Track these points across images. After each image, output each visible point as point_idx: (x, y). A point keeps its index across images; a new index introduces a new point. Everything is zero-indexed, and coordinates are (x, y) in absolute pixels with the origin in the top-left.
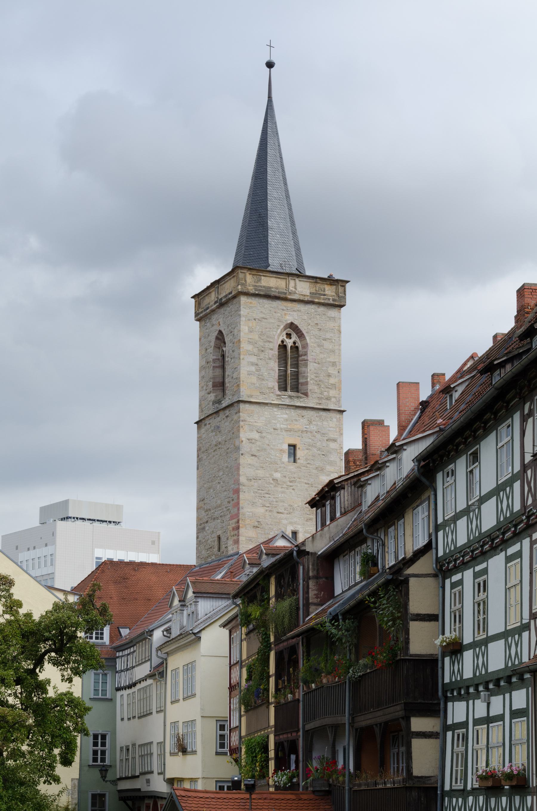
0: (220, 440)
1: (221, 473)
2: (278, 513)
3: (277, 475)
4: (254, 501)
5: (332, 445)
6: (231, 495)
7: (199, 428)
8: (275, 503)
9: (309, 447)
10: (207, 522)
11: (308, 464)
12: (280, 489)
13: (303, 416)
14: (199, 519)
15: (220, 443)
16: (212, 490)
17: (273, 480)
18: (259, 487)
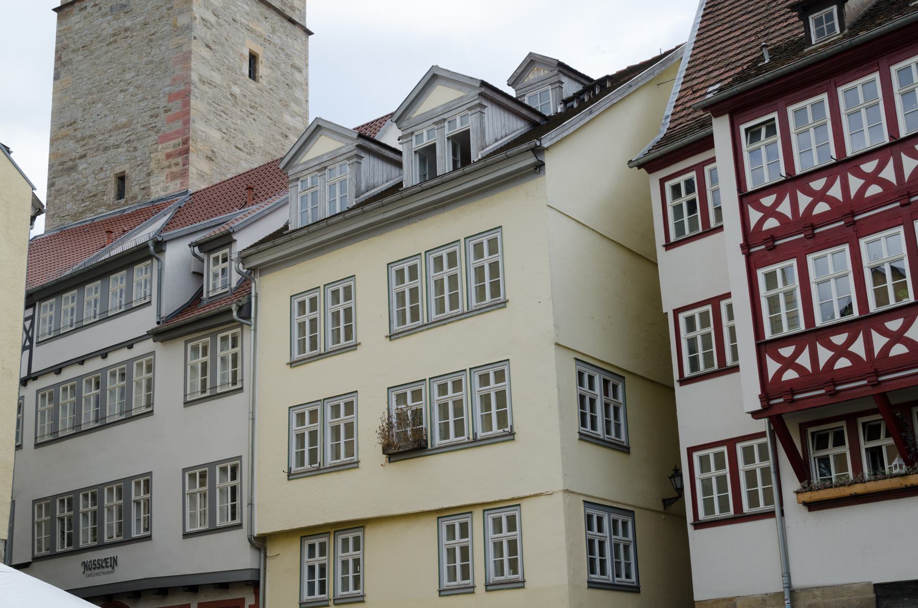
0: (128, 24)
1: (128, 76)
2: (236, 147)
3: (236, 90)
4: (208, 117)
5: (297, 75)
6: (163, 102)
7: (59, 18)
8: (233, 131)
9: (273, 67)
10: (83, 156)
11: (271, 89)
12: (239, 113)
13: (266, 18)
14: (53, 155)
15: (126, 30)
16: (100, 105)
17: (231, 94)
18: (214, 98)
